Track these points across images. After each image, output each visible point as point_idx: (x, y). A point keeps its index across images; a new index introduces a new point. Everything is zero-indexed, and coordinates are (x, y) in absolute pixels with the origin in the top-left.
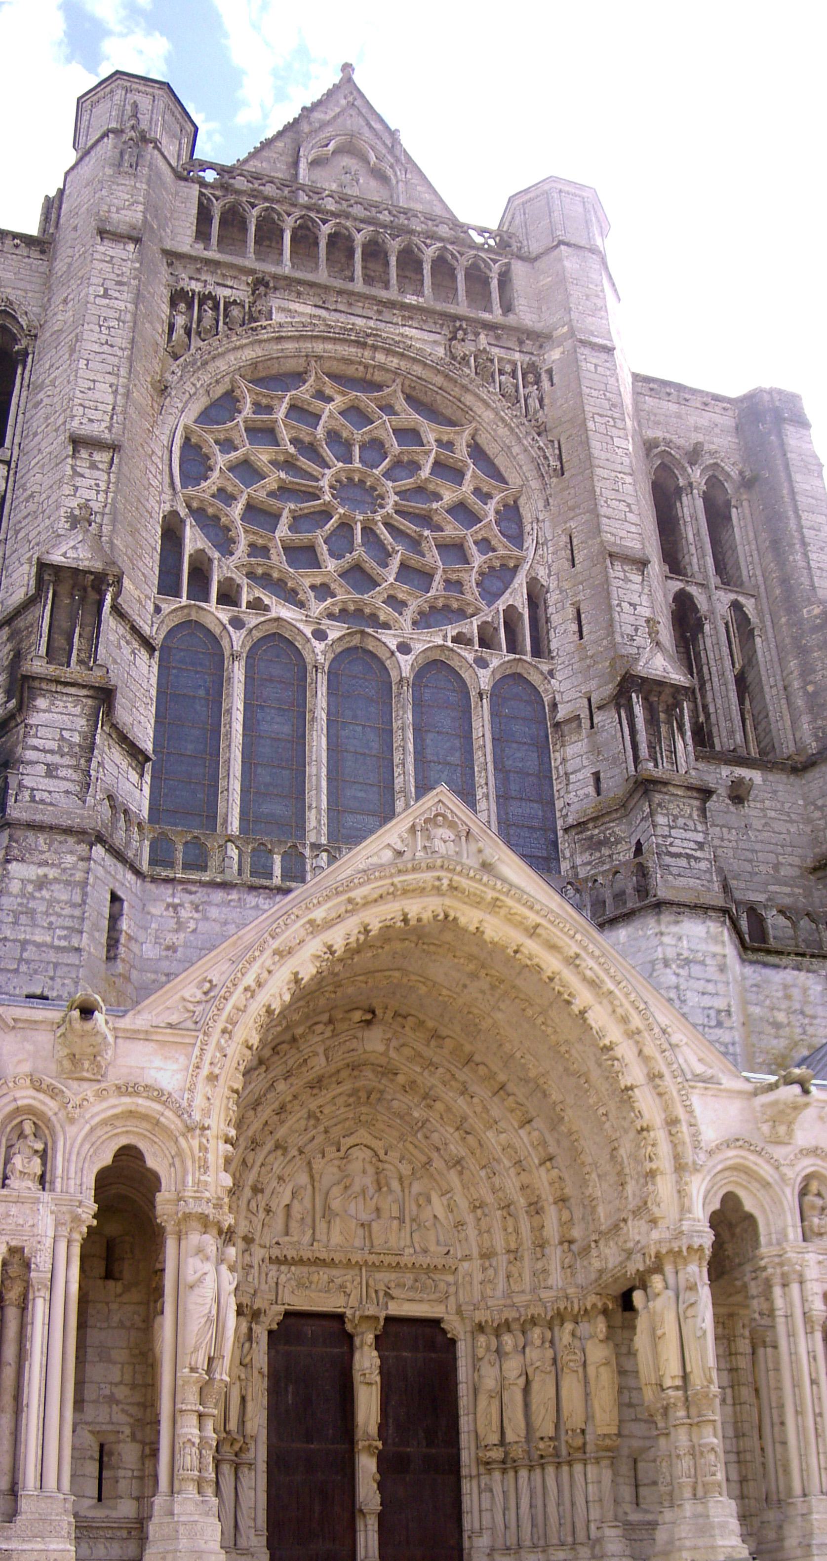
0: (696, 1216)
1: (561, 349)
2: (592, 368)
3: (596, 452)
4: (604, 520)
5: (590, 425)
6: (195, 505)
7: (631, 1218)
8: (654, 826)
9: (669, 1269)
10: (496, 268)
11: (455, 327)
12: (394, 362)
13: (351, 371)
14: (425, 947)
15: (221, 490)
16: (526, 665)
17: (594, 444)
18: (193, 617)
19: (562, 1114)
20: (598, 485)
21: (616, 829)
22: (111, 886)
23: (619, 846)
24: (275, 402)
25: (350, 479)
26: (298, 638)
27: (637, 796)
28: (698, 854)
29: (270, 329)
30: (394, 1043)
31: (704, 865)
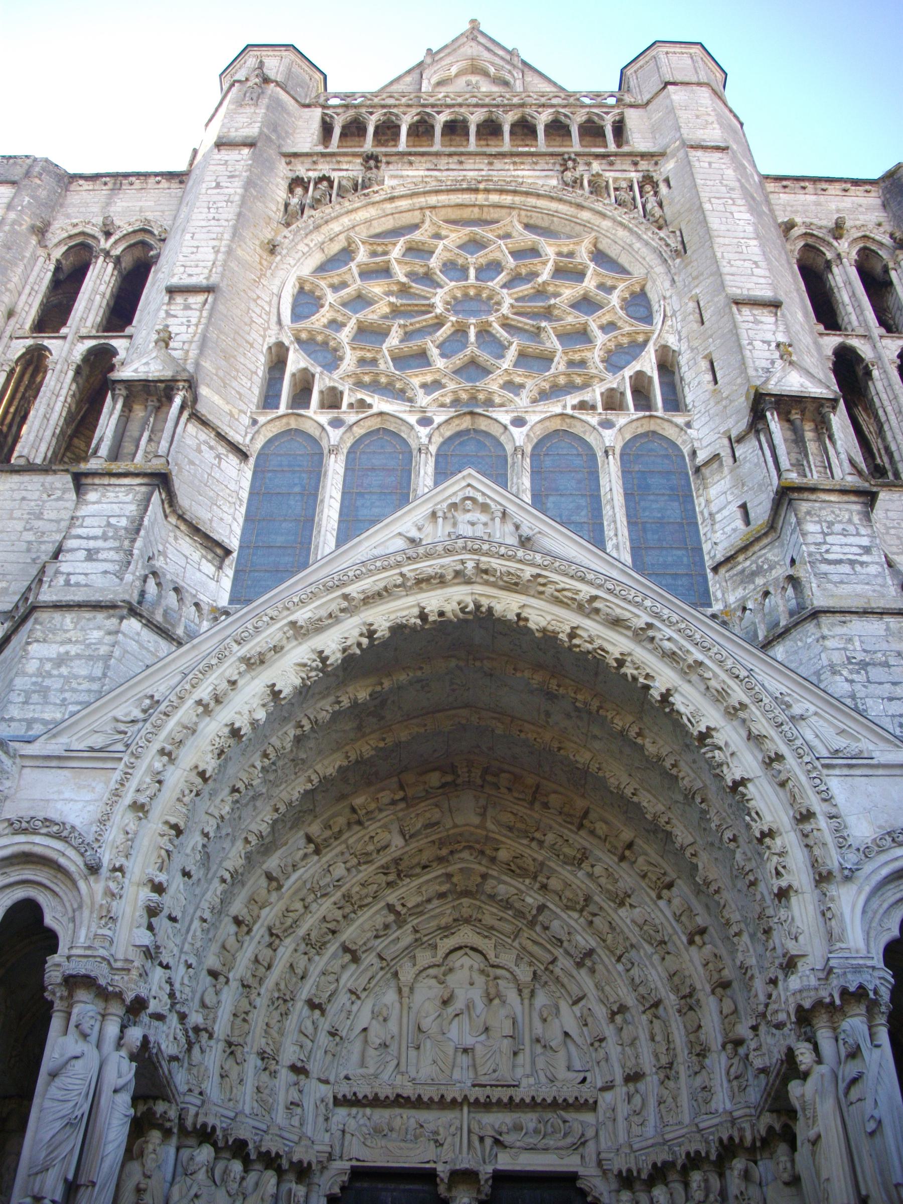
0: (852, 944)
2: (706, 165)
6: (304, 336)
7: (781, 977)
8: (804, 535)
14: (478, 664)
16: (659, 421)
18: (293, 425)
19: (694, 860)
21: (770, 556)
23: (774, 572)
24: (390, 247)
25: (466, 295)
26: (403, 428)
28: (865, 558)
29: (381, 192)
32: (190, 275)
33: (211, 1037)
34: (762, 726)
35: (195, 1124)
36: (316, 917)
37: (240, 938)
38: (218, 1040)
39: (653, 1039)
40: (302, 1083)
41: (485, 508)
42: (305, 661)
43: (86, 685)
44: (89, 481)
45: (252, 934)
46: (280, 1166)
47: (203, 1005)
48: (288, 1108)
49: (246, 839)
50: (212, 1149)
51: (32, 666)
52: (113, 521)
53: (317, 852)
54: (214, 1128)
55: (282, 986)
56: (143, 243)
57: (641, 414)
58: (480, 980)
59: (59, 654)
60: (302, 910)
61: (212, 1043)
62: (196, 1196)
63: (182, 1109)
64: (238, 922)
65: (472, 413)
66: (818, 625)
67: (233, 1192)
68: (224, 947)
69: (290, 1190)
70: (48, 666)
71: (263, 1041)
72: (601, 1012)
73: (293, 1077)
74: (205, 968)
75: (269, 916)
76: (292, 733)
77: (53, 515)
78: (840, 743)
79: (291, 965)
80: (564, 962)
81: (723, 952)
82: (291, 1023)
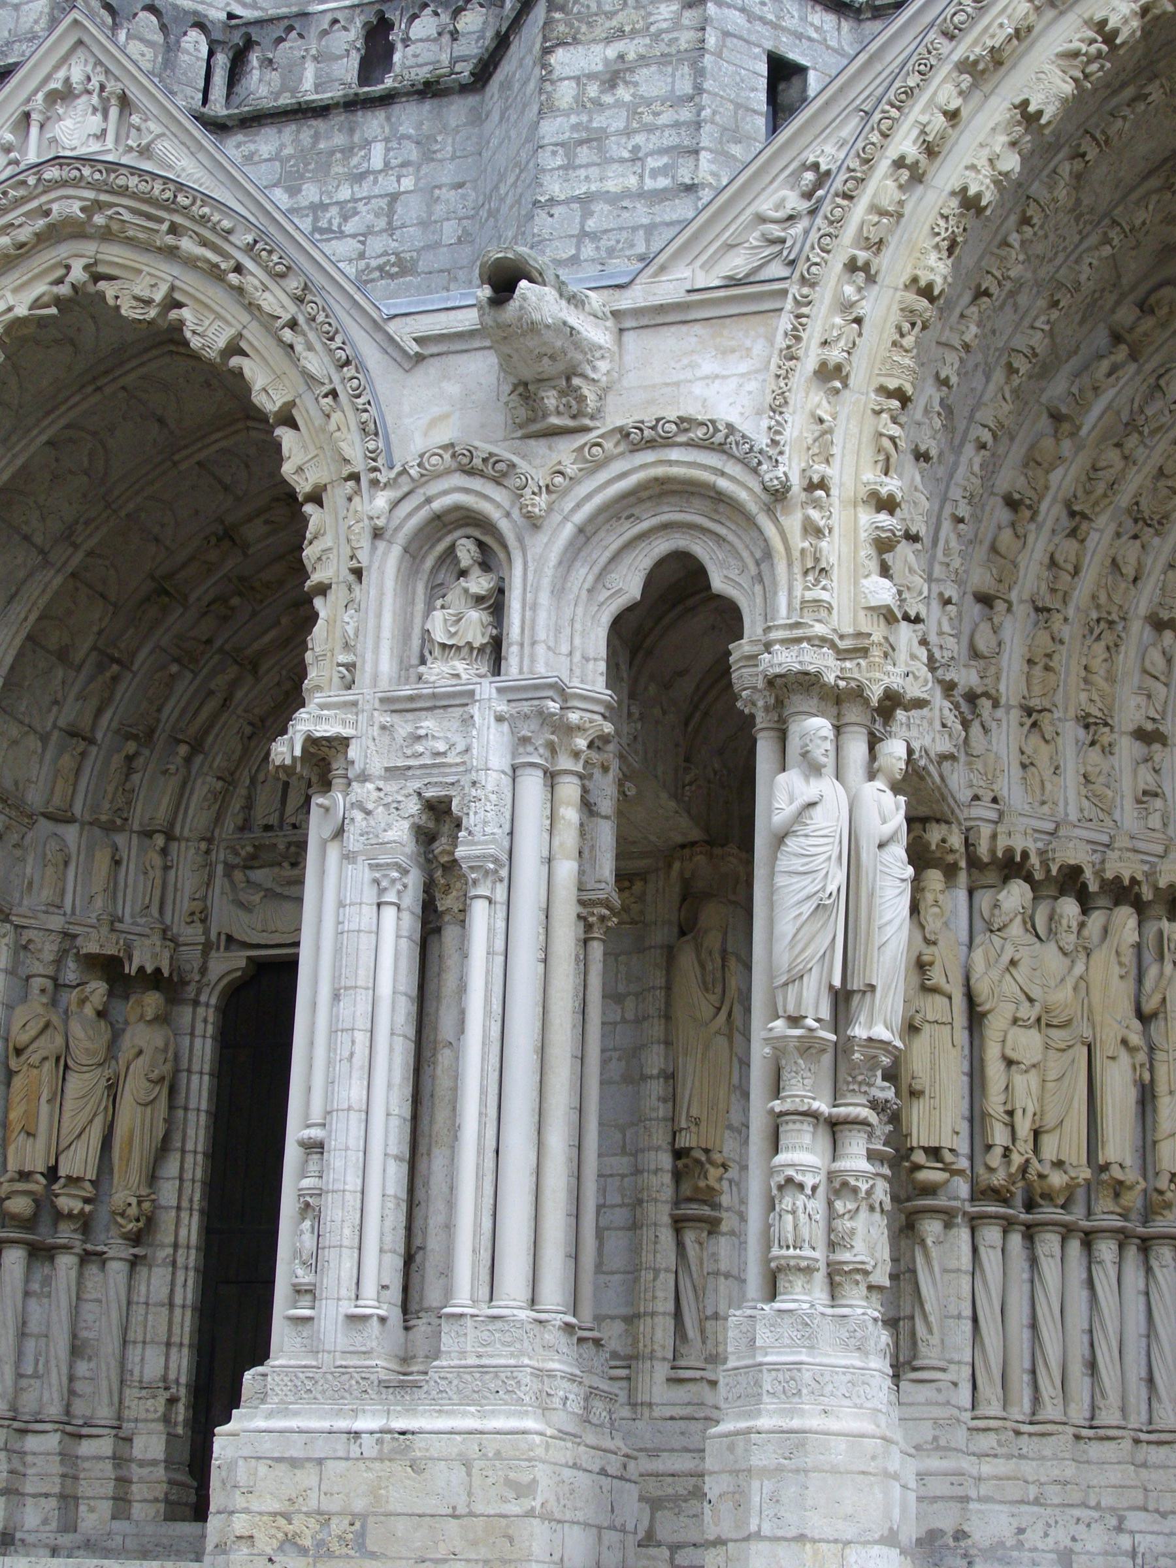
22: (769, 45)
33: (996, 704)
35: (993, 851)
36: (1146, 470)
37: (1021, 531)
38: (1009, 708)
40: (1157, 758)
42: (1076, 45)
43: (666, 118)
45: (1040, 518)
46: (1138, 896)
47: (975, 654)
48: (1139, 802)
49: (1009, 365)
50: (1027, 887)
51: (565, 93)
53: (1133, 356)
54: (1025, 855)
55: (1103, 599)
59: (606, 61)
60: (1119, 464)
61: (1000, 713)
62: (1013, 963)
63: (968, 829)
64: (1012, 504)
67: (1069, 948)
68: (994, 549)
69: (1160, 933)
70: (593, 90)
71: (1083, 696)
73: (1138, 749)
74: (969, 590)
75: (1063, 480)
76: (1066, 169)
79: (1114, 561)
82: (1127, 658)
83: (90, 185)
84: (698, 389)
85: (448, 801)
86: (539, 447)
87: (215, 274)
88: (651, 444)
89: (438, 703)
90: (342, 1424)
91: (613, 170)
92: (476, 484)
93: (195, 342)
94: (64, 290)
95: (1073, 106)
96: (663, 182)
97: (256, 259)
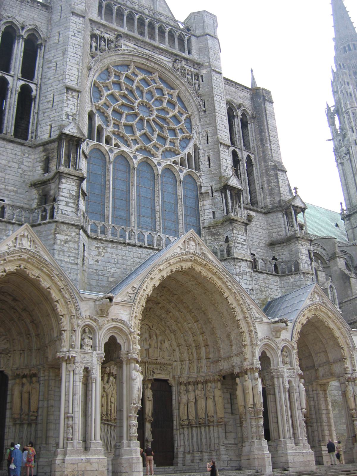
1: (206, 70)
3: (216, 108)
4: (218, 131)
5: (215, 98)
9: (249, 373)
10: (187, 37)
11: (176, 58)
12: (156, 66)
13: (143, 67)
15: (105, 103)
17: (216, 105)
20: (217, 119)
27: (228, 223)
30: (159, 294)
31: (246, 247)
32: (71, 80)
34: (245, 310)
39: (189, 353)
41: (194, 241)
44: (62, 174)
51: (58, 242)
52: (71, 192)
56: (33, 34)
57: (190, 170)
58: (148, 332)
65: (147, 158)
66: (234, 261)
70: (63, 243)
72: (175, 344)
77: (26, 164)
78: (257, 315)
80: (168, 331)
81: (208, 338)
83: (29, 255)
84: (121, 315)
85: (88, 368)
86: (101, 318)
87: (49, 276)
88: (115, 322)
89: (87, 353)
90: (80, 458)
91: (66, 257)
92: (92, 321)
93: (43, 285)
94: (18, 268)
95: (159, 286)
96: (73, 262)
97: (58, 277)
